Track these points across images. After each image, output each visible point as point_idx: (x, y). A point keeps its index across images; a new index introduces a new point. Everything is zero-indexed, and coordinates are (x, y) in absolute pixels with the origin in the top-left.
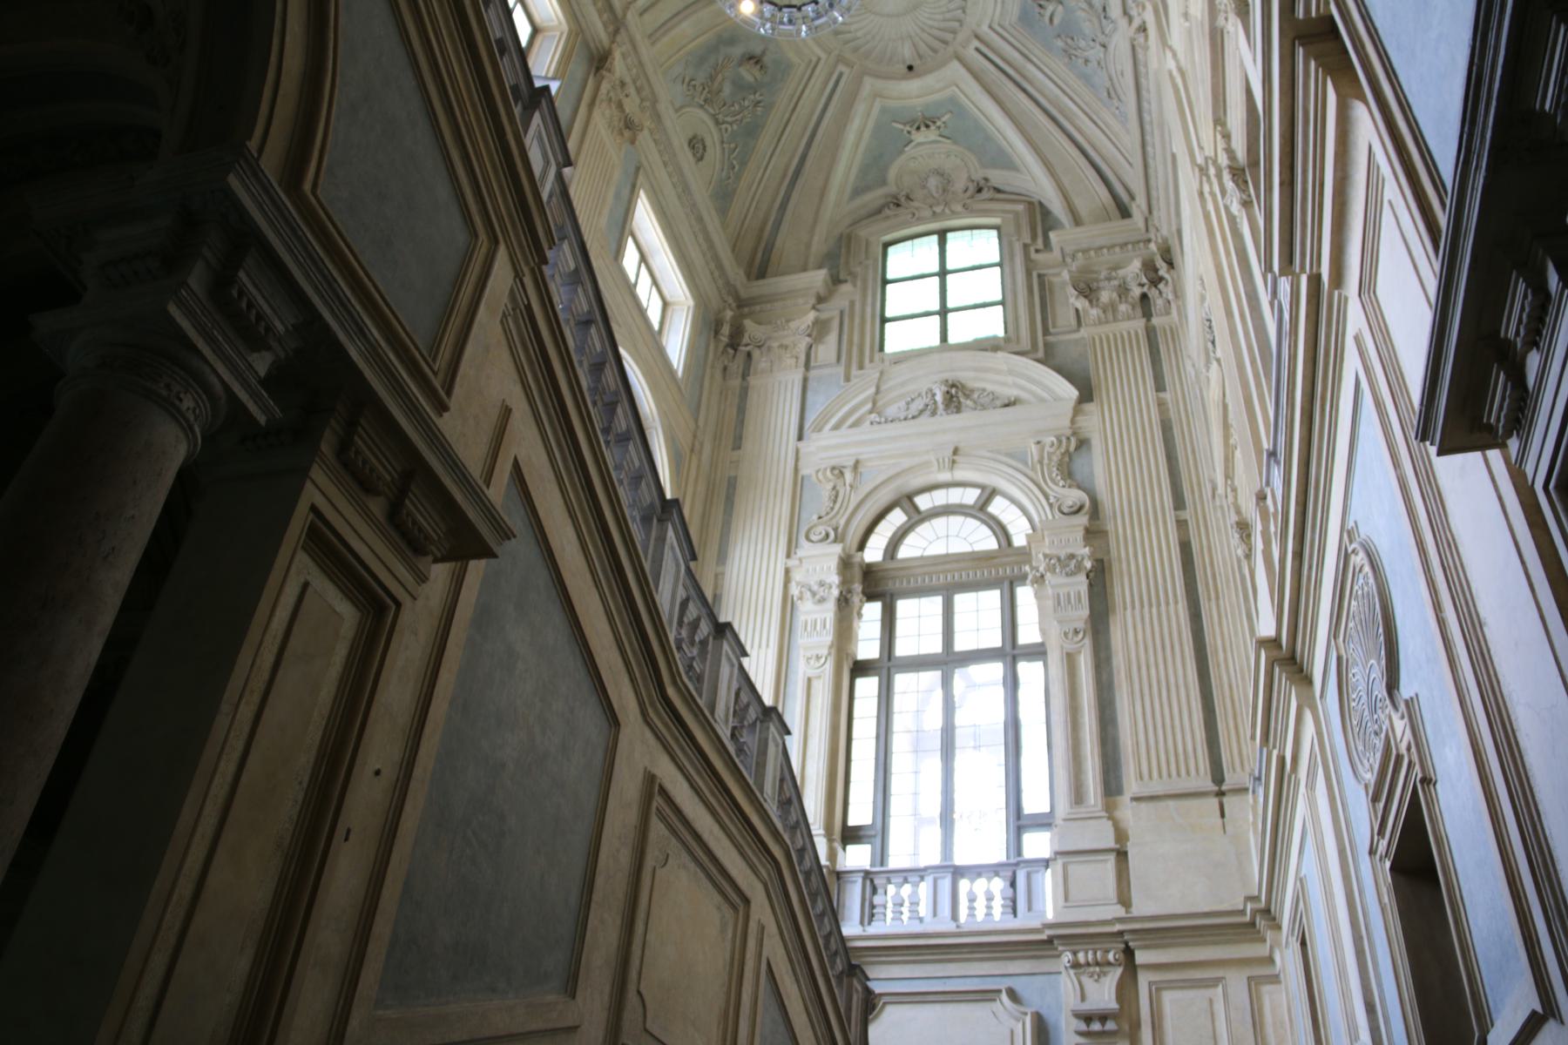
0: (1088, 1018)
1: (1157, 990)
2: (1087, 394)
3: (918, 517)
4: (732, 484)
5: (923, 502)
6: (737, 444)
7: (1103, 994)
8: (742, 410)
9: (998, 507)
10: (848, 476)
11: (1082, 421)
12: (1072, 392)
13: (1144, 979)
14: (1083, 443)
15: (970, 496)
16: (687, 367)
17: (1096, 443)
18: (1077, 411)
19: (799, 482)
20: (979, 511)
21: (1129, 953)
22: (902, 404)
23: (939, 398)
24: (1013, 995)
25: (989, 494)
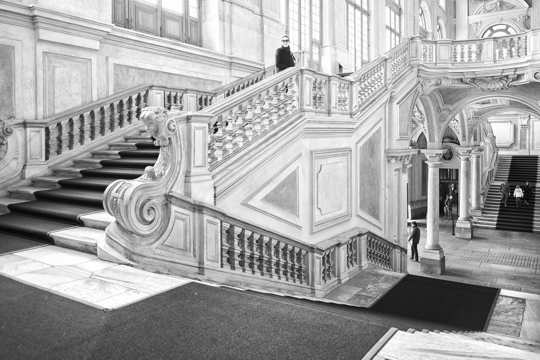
0: (522, 126)
1: (533, 121)
2: (530, 6)
3: (493, 32)
4: (455, 26)
5: (495, 28)
6: (455, 18)
7: (525, 122)
8: (455, 7)
9: (510, 30)
10: (479, 24)
11: (529, 12)
12: (528, 6)
13: (532, 120)
14: (529, 17)
15: (504, 27)
16: (446, 5)
17: (531, 17)
18: (528, 10)
19: (470, 26)
20: (506, 31)
21: (530, 116)
22: (490, 6)
23: (498, 5)
24: (510, 121)
25: (508, 27)
